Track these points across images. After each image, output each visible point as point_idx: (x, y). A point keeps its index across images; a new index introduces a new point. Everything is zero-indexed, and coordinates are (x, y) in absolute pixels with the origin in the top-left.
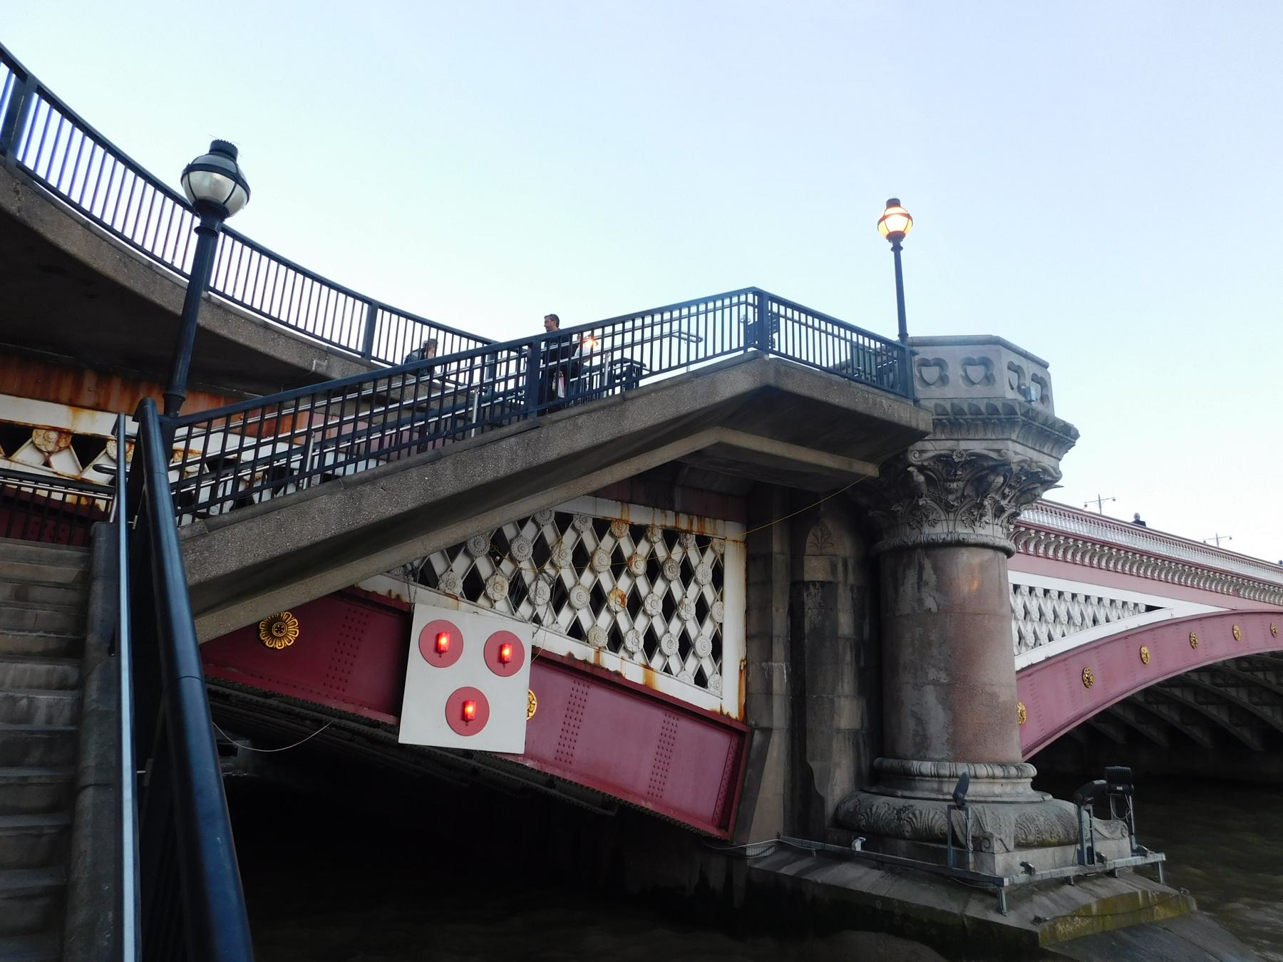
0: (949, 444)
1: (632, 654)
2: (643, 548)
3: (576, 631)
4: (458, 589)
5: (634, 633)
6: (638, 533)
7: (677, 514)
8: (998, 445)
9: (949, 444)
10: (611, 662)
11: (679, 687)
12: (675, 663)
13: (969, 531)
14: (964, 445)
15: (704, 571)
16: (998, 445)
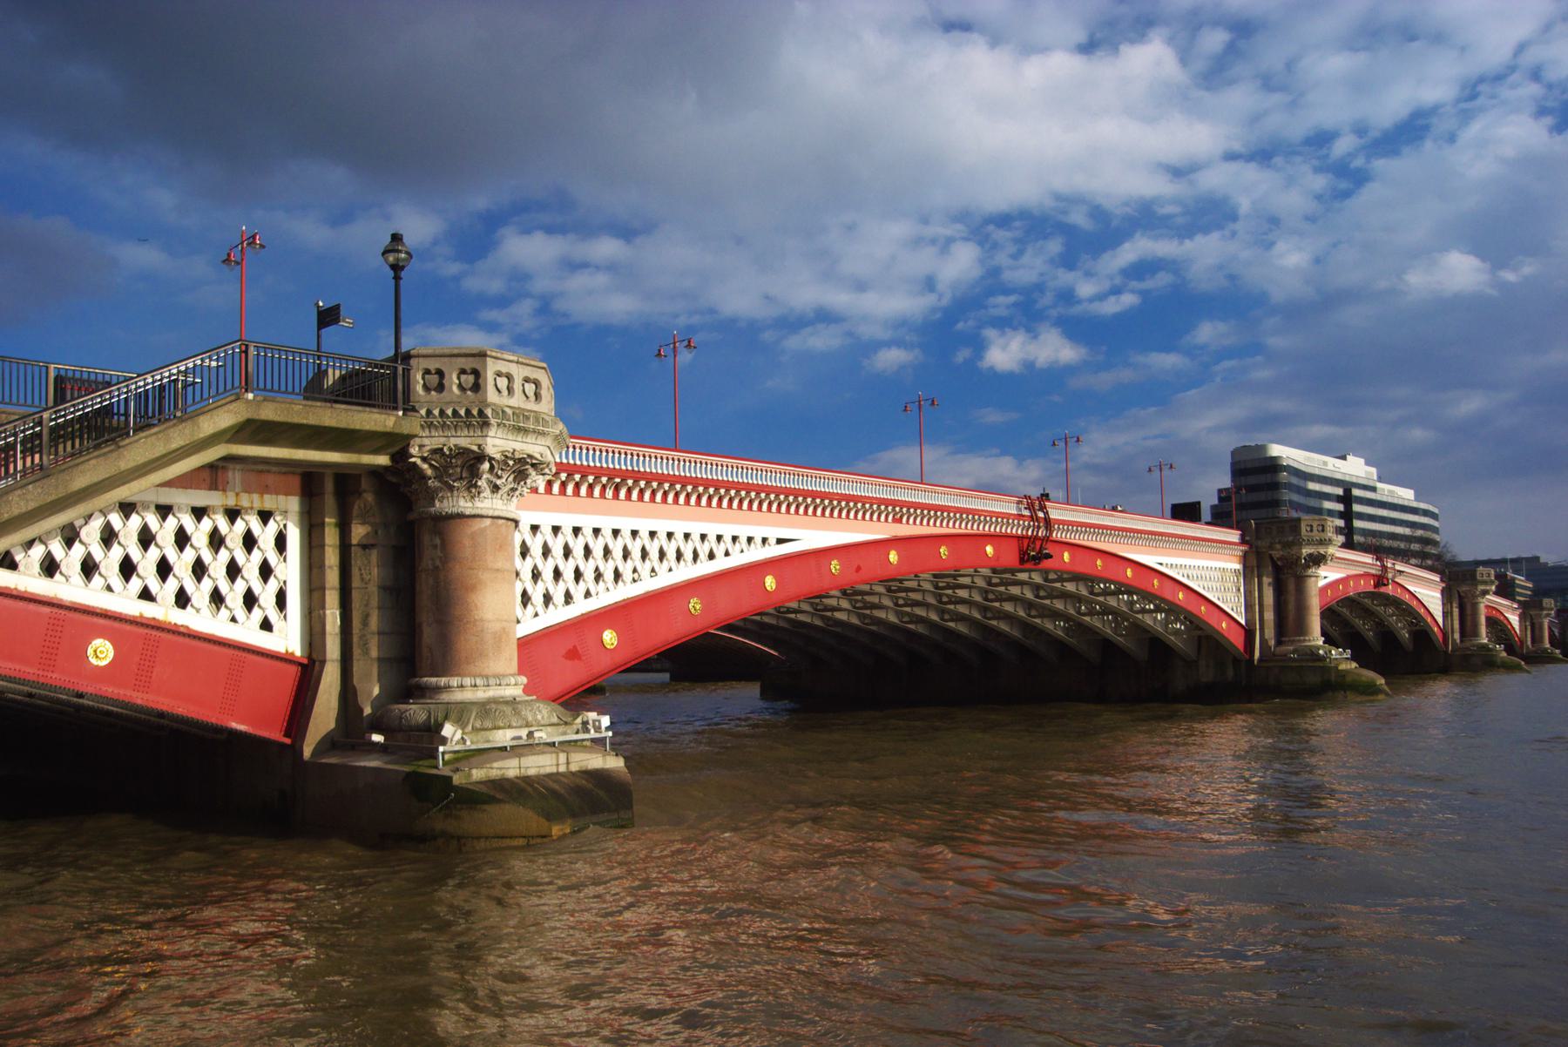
0: (442, 440)
1: (198, 611)
3: (146, 595)
4: (37, 568)
5: (200, 594)
6: (199, 513)
7: (237, 494)
8: (480, 441)
9: (442, 440)
11: (247, 632)
12: (240, 612)
13: (470, 504)
14: (453, 441)
15: (266, 536)
16: (480, 441)
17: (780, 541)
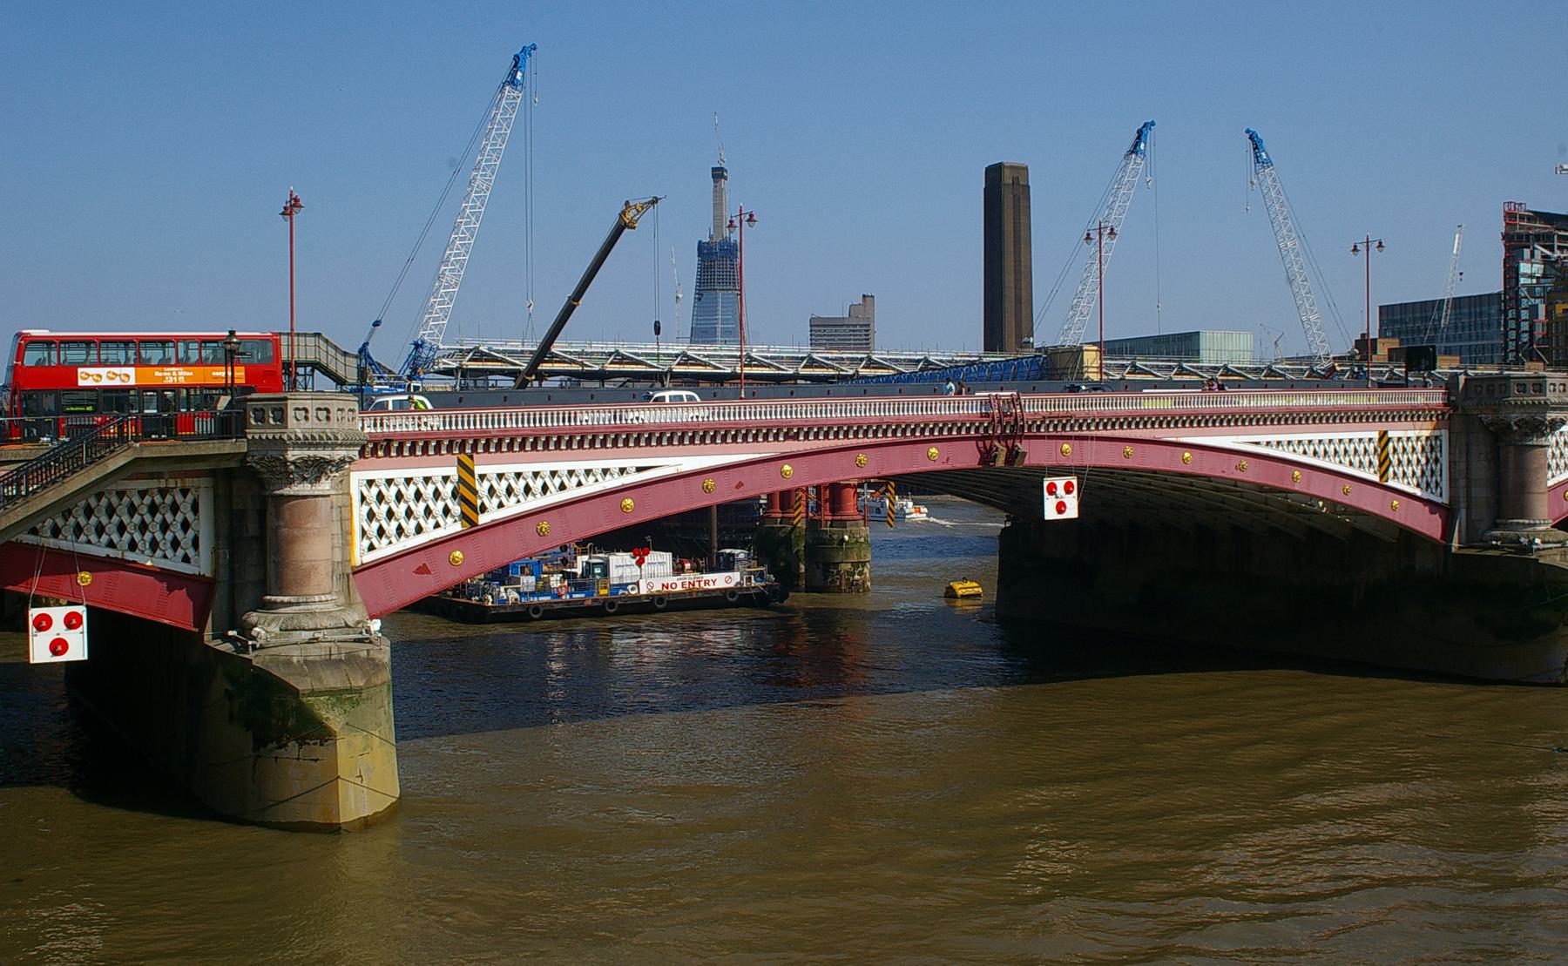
2: (147, 500)
3: (111, 544)
4: (49, 534)
5: (143, 541)
10: (130, 556)
12: (169, 553)
17: (639, 470)
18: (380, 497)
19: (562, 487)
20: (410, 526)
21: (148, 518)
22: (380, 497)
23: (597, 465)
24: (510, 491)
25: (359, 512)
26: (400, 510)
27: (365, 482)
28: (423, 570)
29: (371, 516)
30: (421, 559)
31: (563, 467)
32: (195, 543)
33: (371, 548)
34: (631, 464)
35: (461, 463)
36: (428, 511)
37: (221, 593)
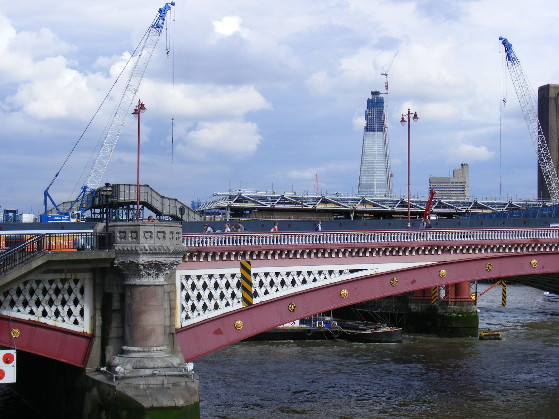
1: (50, 317)
2: (54, 286)
6: (51, 282)
7: (66, 274)
10: (43, 320)
11: (68, 325)
12: (66, 318)
17: (352, 271)
18: (193, 287)
19: (304, 282)
20: (211, 305)
21: (54, 297)
22: (193, 287)
23: (326, 268)
24: (272, 283)
25: (180, 296)
26: (205, 294)
27: (184, 277)
28: (218, 332)
29: (188, 298)
30: (217, 325)
31: (304, 269)
32: (82, 313)
33: (187, 317)
34: (346, 267)
35: (243, 266)
36: (222, 296)
37: (97, 343)
